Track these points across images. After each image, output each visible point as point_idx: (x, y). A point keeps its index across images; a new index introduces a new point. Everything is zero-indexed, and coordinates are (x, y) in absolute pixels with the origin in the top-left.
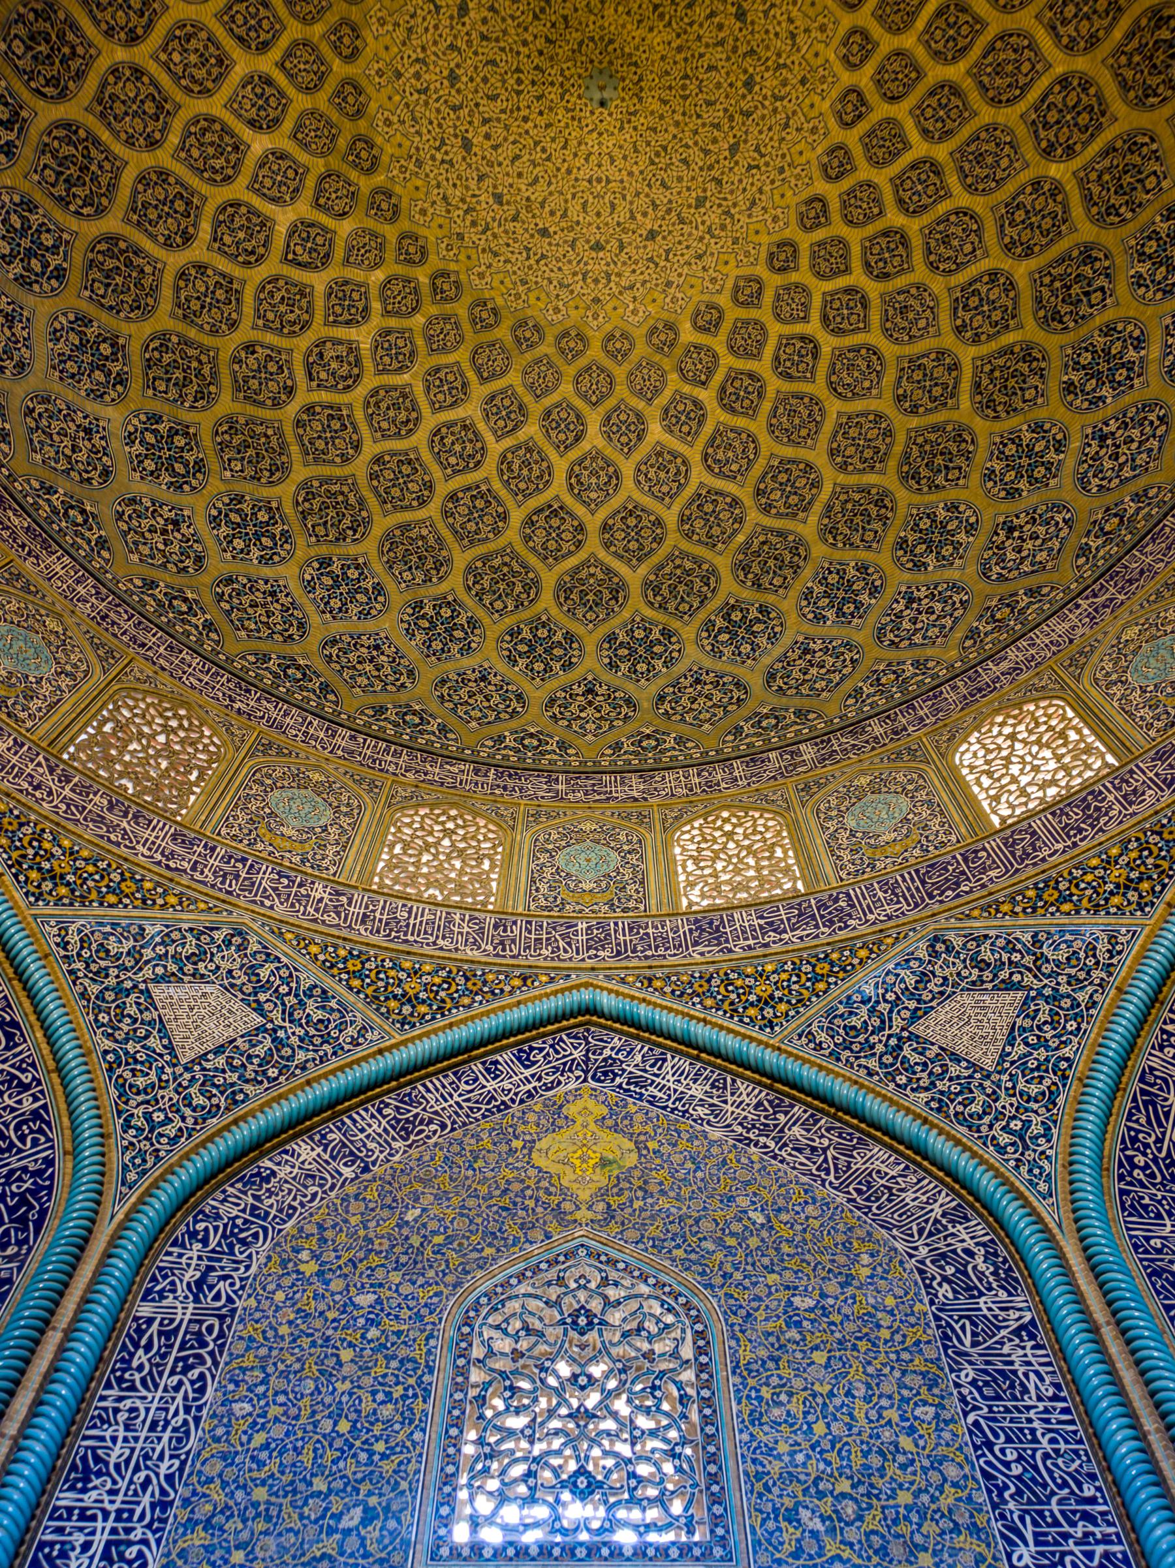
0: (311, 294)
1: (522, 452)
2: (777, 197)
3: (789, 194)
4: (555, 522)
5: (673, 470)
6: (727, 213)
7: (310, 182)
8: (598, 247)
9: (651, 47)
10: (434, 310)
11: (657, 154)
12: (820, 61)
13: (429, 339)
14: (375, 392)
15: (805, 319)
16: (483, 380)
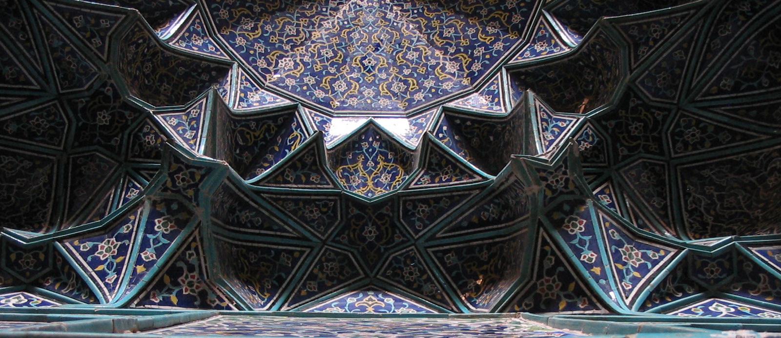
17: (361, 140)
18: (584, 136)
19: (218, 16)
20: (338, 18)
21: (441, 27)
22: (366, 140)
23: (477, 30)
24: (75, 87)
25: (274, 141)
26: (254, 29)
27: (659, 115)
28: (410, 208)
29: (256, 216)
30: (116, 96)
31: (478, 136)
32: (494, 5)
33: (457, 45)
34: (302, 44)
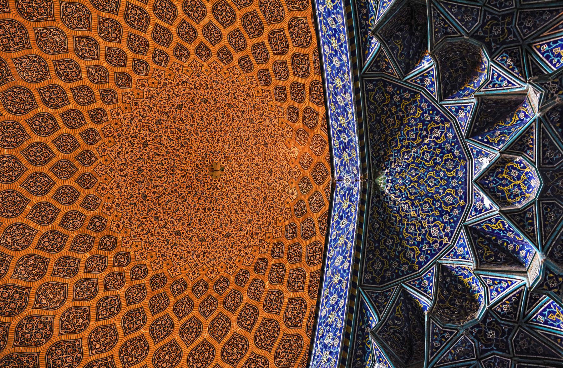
2: (244, 83)
6: (253, 107)
7: (225, 312)
8: (271, 172)
9: (198, 147)
10: (285, 257)
11: (237, 143)
15: (285, 62)
16: (314, 234)
17: (488, 188)
18: (503, 62)
19: (407, 271)
20: (401, 200)
21: (408, 139)
22: (487, 184)
23: (412, 118)
24: (473, 349)
25: (489, 239)
26: (413, 250)
27: (488, 17)
28: (547, 161)
29: (556, 248)
30: (477, 326)
31: (486, 118)
32: (397, 108)
33: (421, 130)
34: (420, 222)
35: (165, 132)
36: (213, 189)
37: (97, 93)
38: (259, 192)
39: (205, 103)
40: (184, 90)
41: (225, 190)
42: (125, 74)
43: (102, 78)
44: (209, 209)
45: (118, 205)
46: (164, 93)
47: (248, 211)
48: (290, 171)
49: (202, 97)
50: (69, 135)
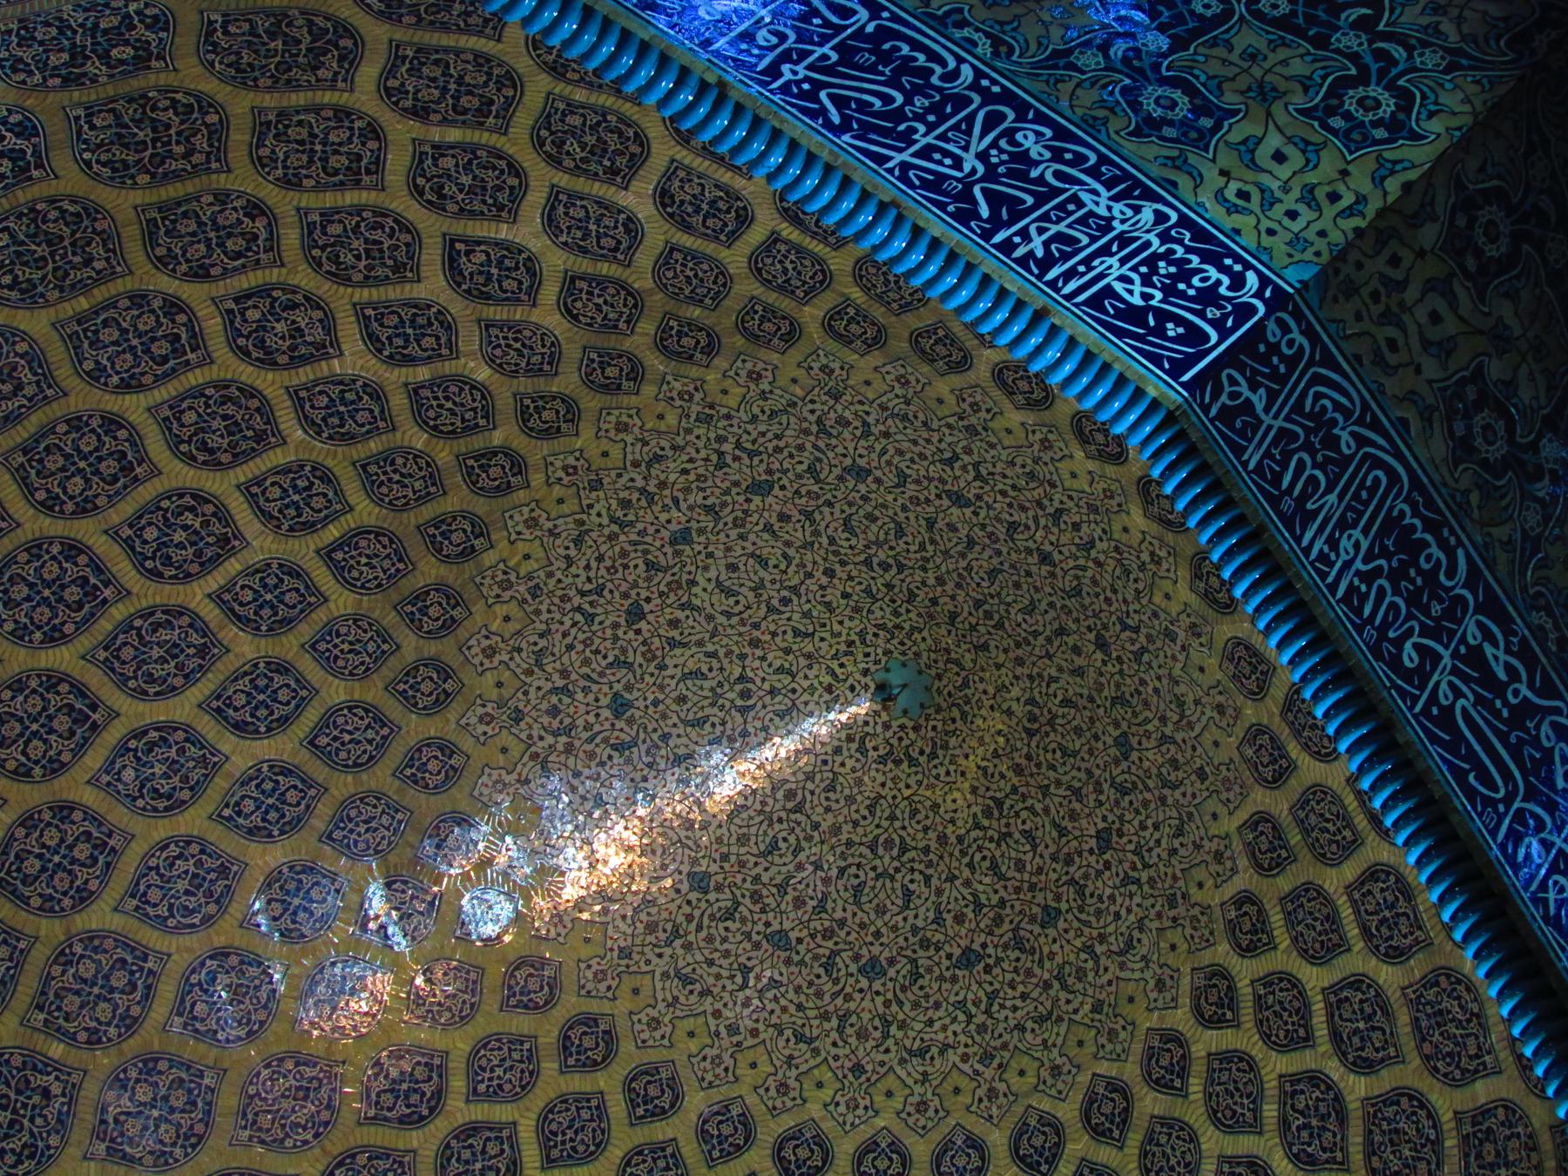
0: (404, 280)
1: (195, 639)
2: (689, 1024)
3: (693, 1046)
4: (62, 723)
5: (192, 903)
6: (676, 933)
7: (605, 268)
8: (620, 707)
11: (790, 795)
12: (879, 1099)
13: (387, 458)
14: (251, 392)
15: (473, 1095)
16: (327, 554)
35: (1040, 870)
36: (897, 627)
37: (1196, 1085)
38: (675, 633)
39: (874, 960)
40: (930, 1022)
41: (847, 623)
42: (1099, 1133)
43: (1163, 1139)
44: (885, 567)
45: (1170, 636)
46: (1002, 1025)
47: (706, 568)
48: (518, 721)
49: (877, 986)
50: (1304, 953)
